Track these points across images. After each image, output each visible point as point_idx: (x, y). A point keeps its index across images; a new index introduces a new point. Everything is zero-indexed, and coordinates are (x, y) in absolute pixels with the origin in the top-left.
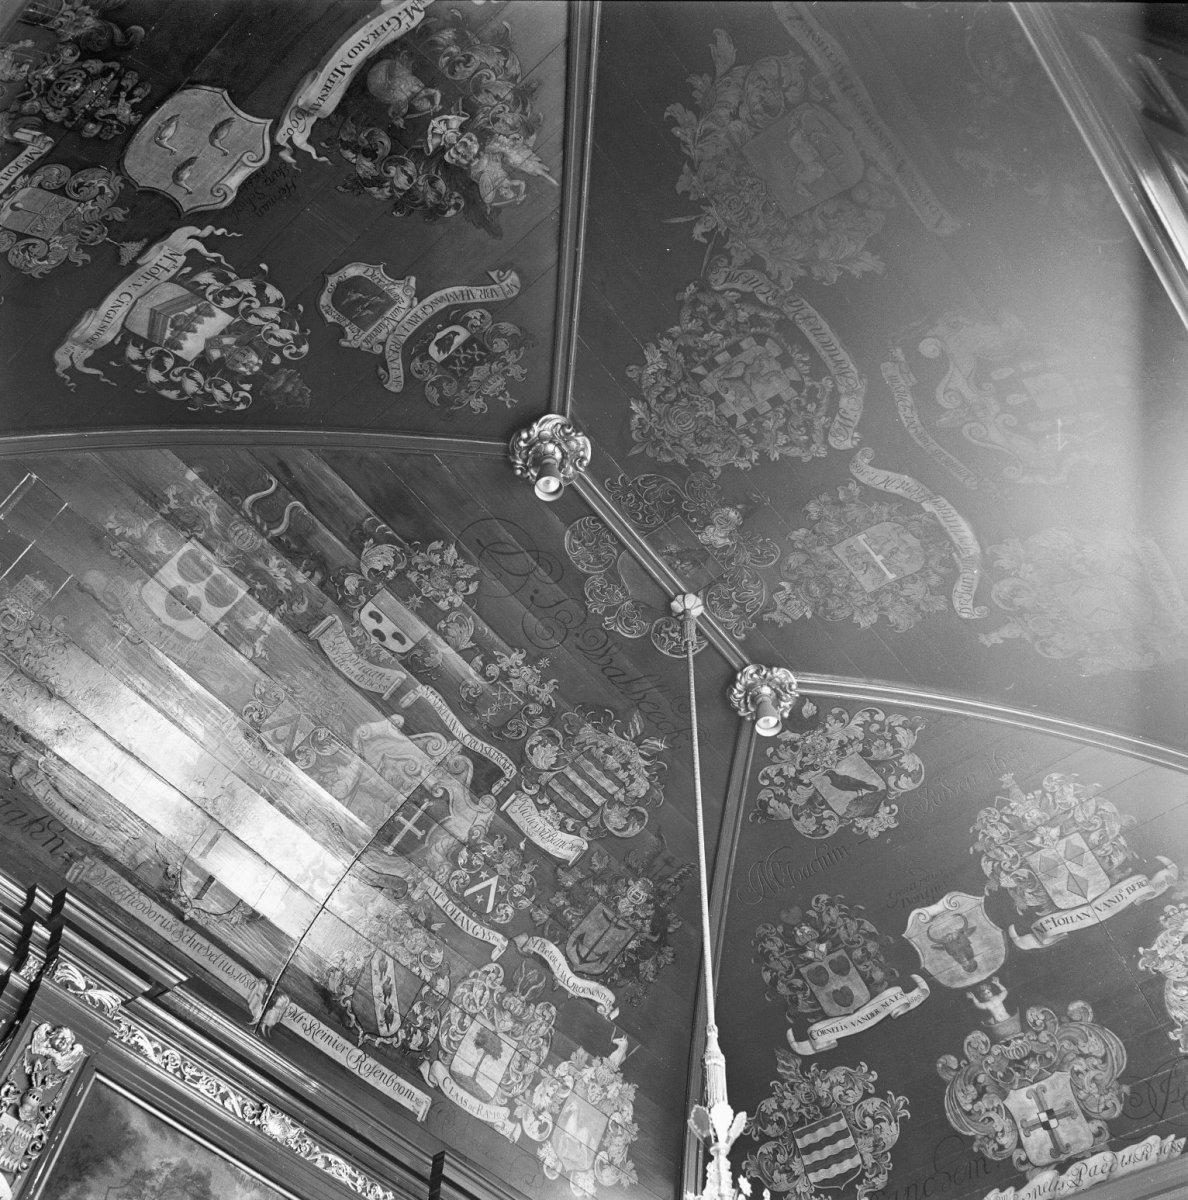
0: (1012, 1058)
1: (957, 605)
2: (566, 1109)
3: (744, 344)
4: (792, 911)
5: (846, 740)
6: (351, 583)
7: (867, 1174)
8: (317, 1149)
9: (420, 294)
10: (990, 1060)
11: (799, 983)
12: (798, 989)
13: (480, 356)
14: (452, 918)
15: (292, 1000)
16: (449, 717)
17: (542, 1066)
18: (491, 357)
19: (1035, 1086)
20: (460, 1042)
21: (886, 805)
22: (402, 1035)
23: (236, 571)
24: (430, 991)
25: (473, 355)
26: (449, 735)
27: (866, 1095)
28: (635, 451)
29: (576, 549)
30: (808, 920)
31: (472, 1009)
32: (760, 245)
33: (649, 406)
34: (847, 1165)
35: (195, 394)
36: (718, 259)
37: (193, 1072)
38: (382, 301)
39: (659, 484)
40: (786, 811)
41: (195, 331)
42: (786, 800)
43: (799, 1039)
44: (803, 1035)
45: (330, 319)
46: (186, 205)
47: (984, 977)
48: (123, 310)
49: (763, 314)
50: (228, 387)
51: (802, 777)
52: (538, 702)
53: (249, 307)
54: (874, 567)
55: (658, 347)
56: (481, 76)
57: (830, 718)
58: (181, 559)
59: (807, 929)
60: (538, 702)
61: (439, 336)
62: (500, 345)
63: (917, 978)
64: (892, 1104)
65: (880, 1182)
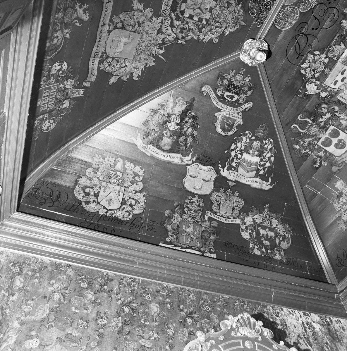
3: (188, 16)
6: (324, 95)
9: (219, 110)
13: (231, 86)
18: (230, 82)
23: (326, 130)
25: (232, 88)
28: (243, 24)
29: (290, 23)
32: (154, 34)
33: (225, 29)
35: (271, 153)
36: (166, 41)
38: (225, 119)
39: (252, 8)
41: (251, 160)
45: (236, 130)
46: (215, 176)
48: (249, 179)
49: (174, 18)
50: (266, 146)
53: (239, 151)
55: (204, 38)
56: (156, 124)
58: (325, 146)
61: (229, 100)
62: (226, 82)
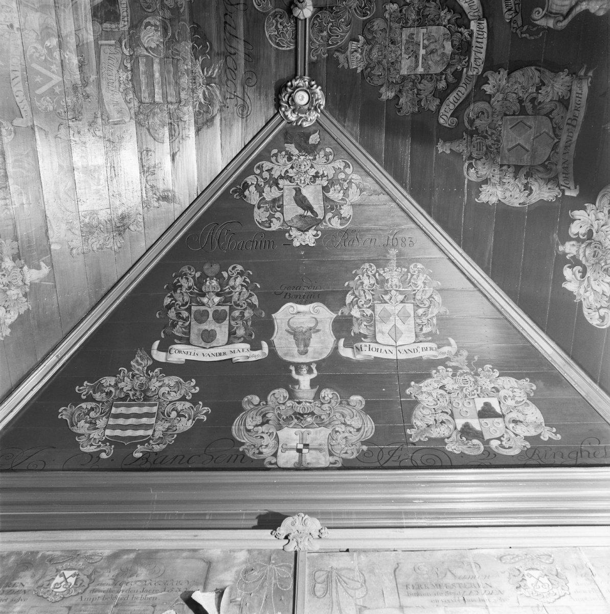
0: (298, 411)
1: (442, 111)
4: (213, 266)
5: (321, 173)
7: (151, 442)
10: (282, 407)
11: (185, 314)
12: (182, 318)
19: (303, 430)
21: (315, 229)
27: (183, 399)
30: (219, 276)
34: (140, 433)
42: (260, 190)
43: (160, 349)
44: (163, 348)
47: (308, 360)
51: (281, 182)
54: (416, 56)
57: (322, 153)
59: (214, 283)
63: (265, 345)
64: (198, 409)
65: (157, 448)
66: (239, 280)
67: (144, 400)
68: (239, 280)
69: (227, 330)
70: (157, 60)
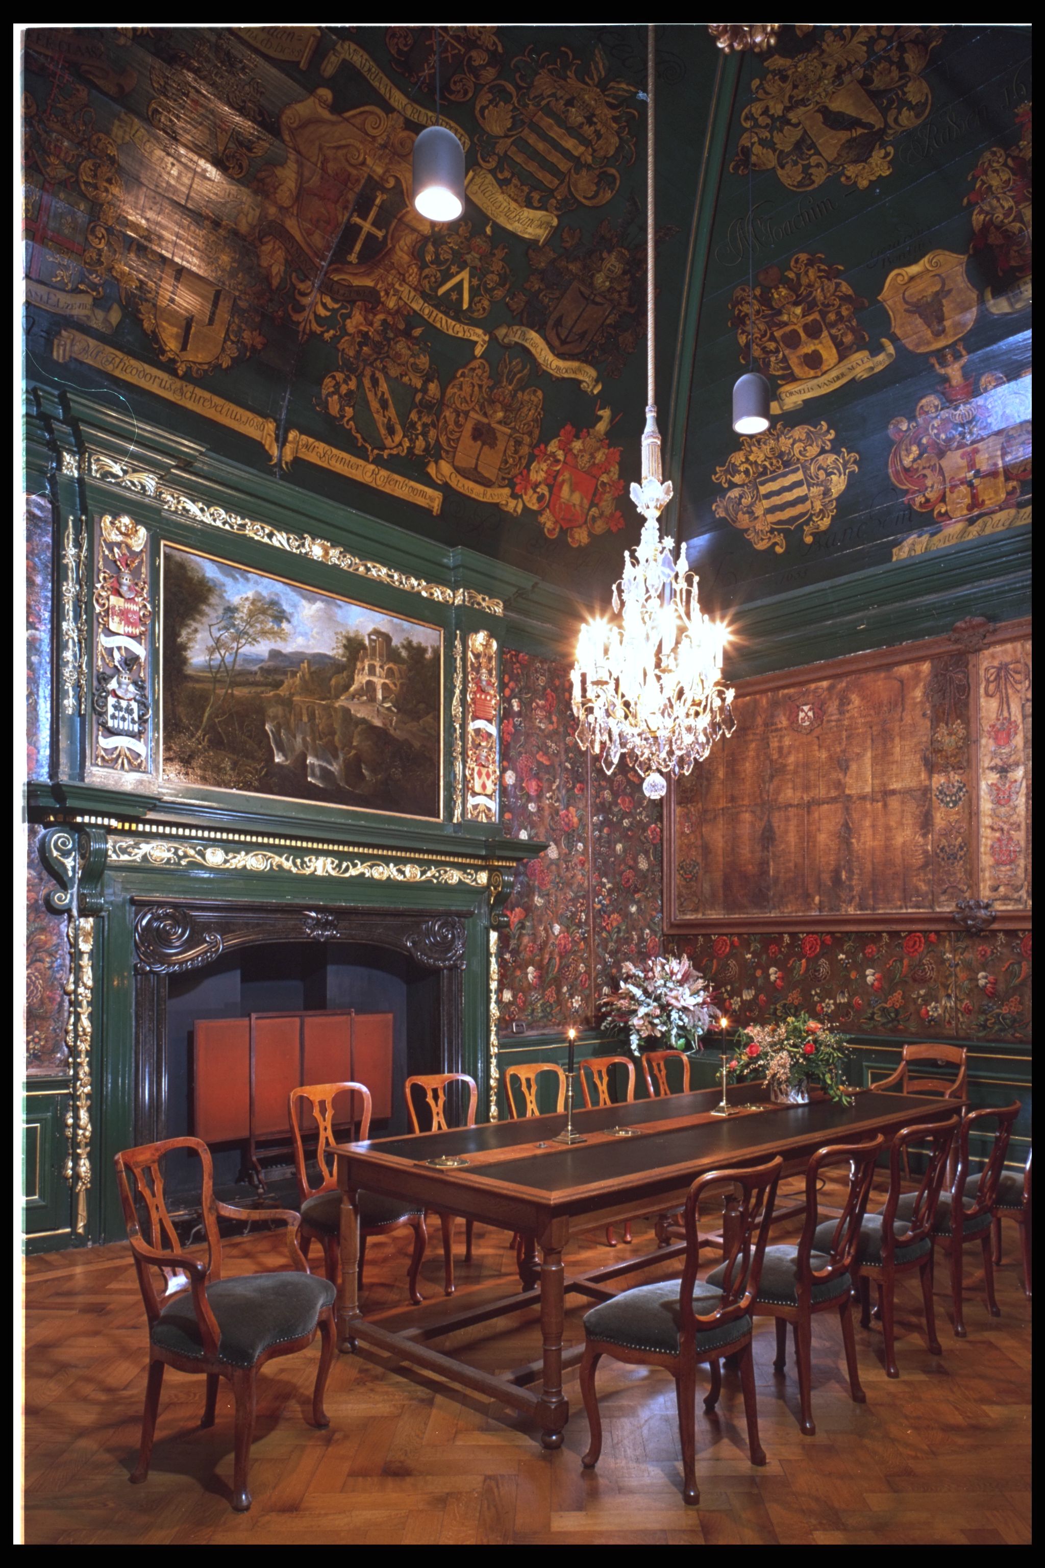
2: (560, 479)
8: (357, 561)
11: (772, 346)
12: (771, 352)
14: (431, 320)
15: (301, 433)
16: (382, 84)
17: (533, 446)
20: (458, 439)
22: (407, 444)
24: (423, 398)
26: (388, 109)
31: (464, 407)
37: (239, 521)
40: (770, 159)
52: (480, 47)
59: (784, 292)
60: (480, 47)
66: (812, 273)
67: (785, 467)
68: (812, 273)
69: (830, 343)
70: (527, 131)
